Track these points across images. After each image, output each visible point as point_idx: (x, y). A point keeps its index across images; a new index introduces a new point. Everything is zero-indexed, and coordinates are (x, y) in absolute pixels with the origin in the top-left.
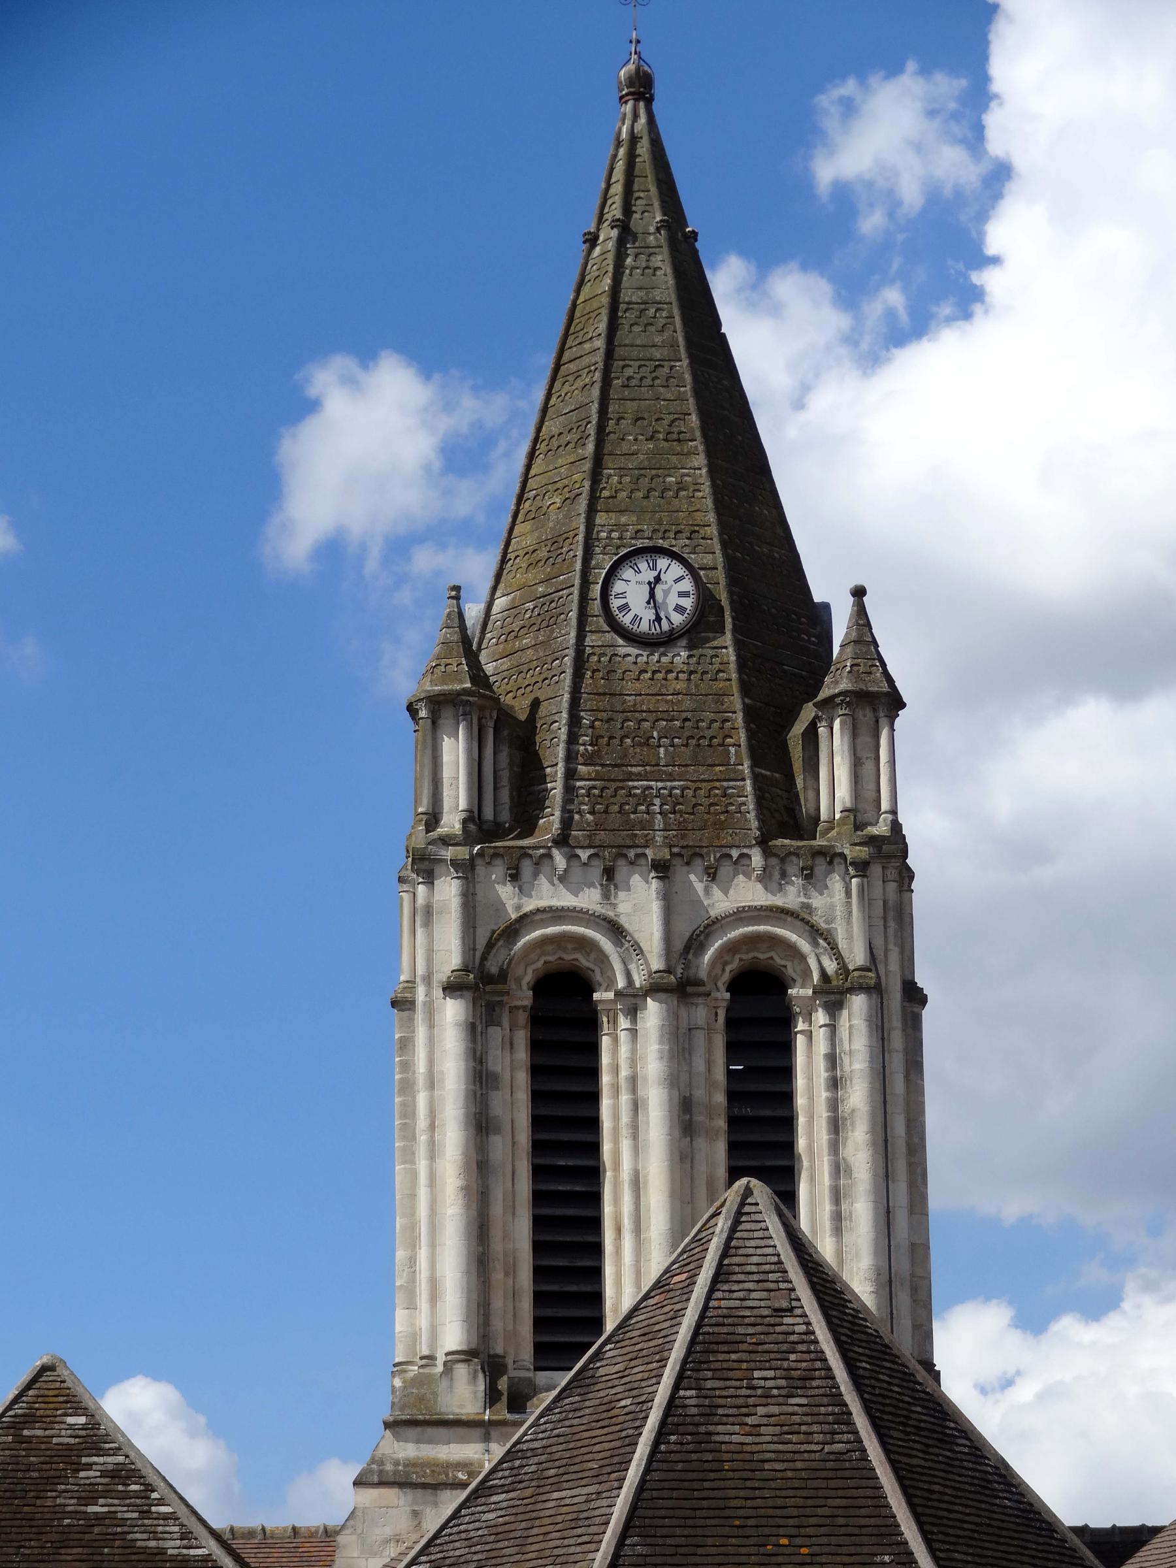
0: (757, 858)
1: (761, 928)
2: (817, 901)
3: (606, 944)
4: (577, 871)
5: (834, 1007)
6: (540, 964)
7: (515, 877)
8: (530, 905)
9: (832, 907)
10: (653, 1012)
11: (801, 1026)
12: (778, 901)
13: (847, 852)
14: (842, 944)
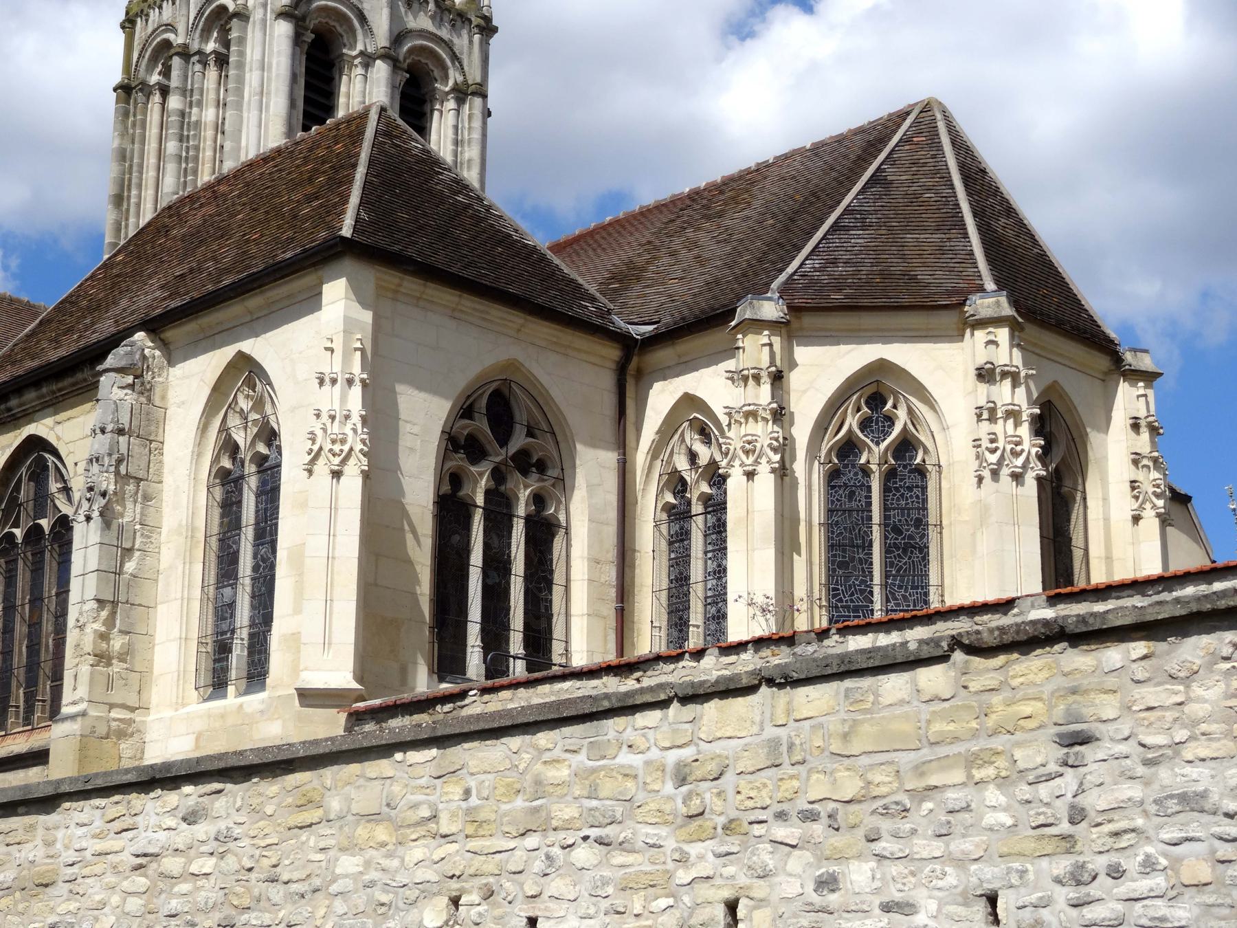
1: (430, 44)
2: (456, 40)
5: (460, 101)
6: (317, 22)
9: (462, 46)
10: (381, 69)
11: (438, 107)
12: (439, 33)
13: (473, 19)
14: (466, 68)
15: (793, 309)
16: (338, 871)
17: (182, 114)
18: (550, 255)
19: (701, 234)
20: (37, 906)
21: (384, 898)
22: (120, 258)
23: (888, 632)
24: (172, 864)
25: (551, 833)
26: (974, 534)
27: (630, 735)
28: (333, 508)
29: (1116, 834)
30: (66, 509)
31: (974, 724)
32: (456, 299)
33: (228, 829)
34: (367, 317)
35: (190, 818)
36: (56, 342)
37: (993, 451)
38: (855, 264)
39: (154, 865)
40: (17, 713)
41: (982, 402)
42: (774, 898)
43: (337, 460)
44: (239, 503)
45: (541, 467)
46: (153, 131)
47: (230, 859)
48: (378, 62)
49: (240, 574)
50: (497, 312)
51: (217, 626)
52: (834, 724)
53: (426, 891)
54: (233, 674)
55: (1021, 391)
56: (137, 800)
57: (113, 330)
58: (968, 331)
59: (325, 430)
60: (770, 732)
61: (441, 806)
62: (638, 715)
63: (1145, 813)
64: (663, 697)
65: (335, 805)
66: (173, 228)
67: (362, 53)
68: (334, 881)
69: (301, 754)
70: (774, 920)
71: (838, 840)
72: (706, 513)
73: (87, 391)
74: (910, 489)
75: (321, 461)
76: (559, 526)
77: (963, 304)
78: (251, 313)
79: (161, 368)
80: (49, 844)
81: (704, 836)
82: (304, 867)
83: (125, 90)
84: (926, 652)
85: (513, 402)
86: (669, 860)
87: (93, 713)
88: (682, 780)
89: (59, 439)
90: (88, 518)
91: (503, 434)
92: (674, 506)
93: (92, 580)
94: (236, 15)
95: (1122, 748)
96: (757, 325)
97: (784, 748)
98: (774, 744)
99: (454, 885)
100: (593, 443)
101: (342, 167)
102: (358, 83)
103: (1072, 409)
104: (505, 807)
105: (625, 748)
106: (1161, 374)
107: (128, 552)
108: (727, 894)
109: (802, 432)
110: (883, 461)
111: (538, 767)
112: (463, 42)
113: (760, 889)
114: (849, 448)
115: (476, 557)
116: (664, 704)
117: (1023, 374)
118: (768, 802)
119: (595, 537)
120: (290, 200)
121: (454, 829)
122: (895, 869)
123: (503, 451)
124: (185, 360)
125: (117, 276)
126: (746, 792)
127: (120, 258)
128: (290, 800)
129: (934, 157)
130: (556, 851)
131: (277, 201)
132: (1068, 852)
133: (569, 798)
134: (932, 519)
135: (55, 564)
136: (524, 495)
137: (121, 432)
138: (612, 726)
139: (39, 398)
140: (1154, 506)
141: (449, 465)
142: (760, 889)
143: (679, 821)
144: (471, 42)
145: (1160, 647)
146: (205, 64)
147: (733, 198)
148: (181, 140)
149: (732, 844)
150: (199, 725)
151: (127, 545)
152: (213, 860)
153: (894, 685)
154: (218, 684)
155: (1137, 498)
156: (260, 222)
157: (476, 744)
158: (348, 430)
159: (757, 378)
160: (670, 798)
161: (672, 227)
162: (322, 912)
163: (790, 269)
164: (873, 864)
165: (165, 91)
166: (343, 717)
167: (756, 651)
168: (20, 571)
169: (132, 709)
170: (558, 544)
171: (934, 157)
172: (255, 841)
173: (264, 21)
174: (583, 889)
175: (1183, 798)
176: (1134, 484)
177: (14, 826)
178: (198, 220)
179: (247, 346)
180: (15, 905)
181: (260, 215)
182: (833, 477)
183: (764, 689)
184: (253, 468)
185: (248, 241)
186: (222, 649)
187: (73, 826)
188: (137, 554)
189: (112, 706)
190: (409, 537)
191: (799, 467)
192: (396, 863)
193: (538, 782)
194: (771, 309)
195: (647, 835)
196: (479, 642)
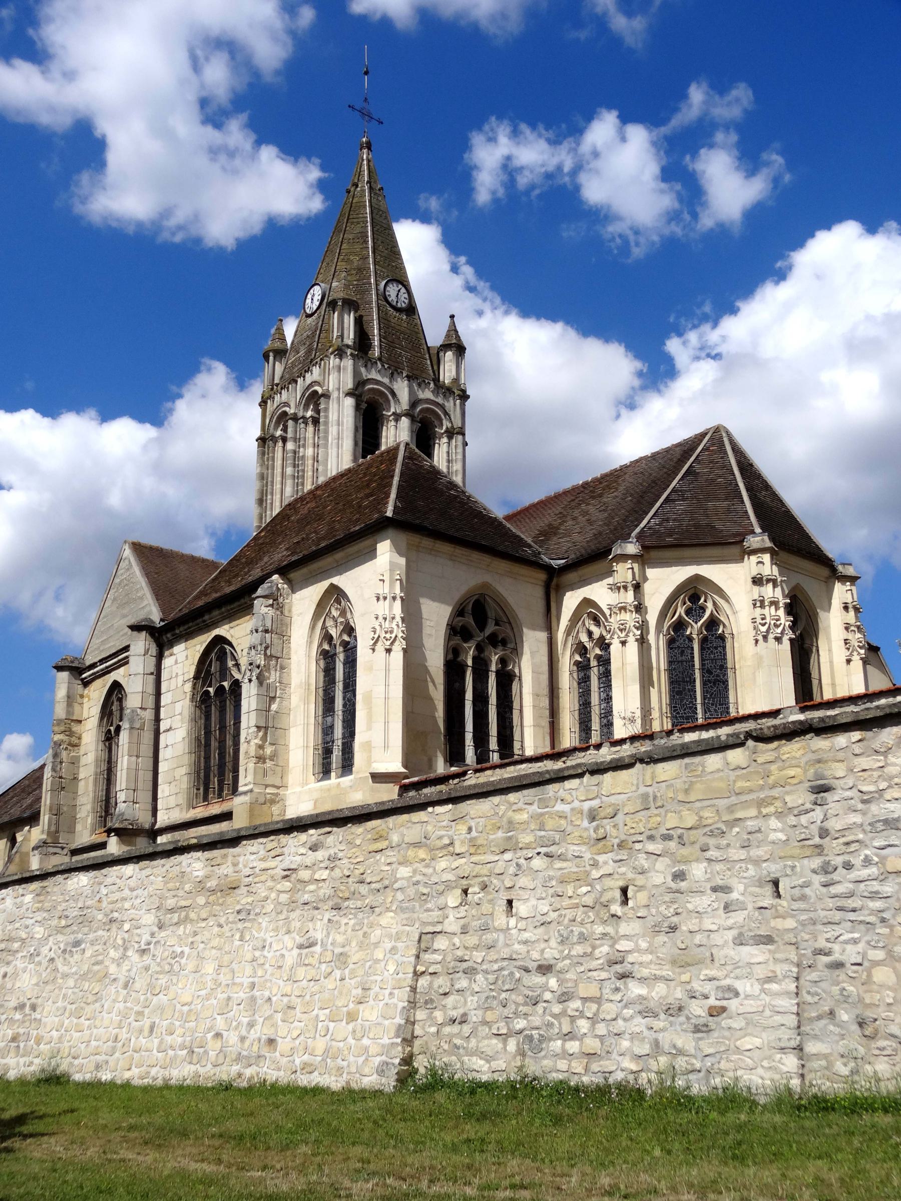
0: (432, 385)
2: (446, 404)
3: (390, 397)
4: (383, 371)
5: (450, 438)
7: (366, 366)
8: (370, 377)
10: (405, 422)
12: (436, 400)
15: (645, 548)
16: (398, 876)
17: (295, 452)
18: (504, 522)
19: (590, 507)
20: (230, 900)
21: (425, 891)
22: (263, 534)
23: (707, 730)
24: (304, 874)
25: (519, 851)
26: (754, 673)
27: (562, 794)
28: (387, 670)
29: (847, 844)
30: (237, 676)
31: (761, 782)
32: (452, 549)
33: (335, 854)
34: (402, 561)
35: (314, 848)
36: (229, 583)
37: (763, 625)
38: (679, 521)
39: (294, 875)
40: (214, 792)
41: (756, 597)
42: (649, 885)
43: (388, 643)
44: (334, 669)
45: (504, 642)
46: (278, 463)
47: (337, 871)
48: (403, 418)
49: (336, 709)
50: (476, 556)
51: (324, 739)
52: (679, 784)
53: (449, 886)
54: (334, 766)
55: (778, 590)
56: (283, 838)
57: (260, 574)
58: (746, 557)
59: (381, 626)
60: (643, 790)
61: (455, 837)
62: (566, 782)
63: (864, 831)
64: (580, 771)
65: (395, 838)
66: (292, 516)
67: (394, 414)
68: (396, 882)
69: (375, 810)
70: (649, 898)
71: (684, 851)
72: (599, 666)
73: (247, 609)
74: (716, 648)
75: (380, 643)
76: (515, 676)
77: (743, 541)
78: (337, 562)
79: (288, 595)
80: (235, 865)
81: (606, 851)
82: (379, 874)
83: (263, 440)
84: (731, 741)
85: (487, 607)
86: (587, 865)
87: (256, 790)
88: (593, 819)
89: (232, 636)
90: (250, 681)
91: (481, 624)
92: (580, 662)
93: (253, 715)
94: (323, 395)
95: (849, 794)
96: (624, 557)
97: (651, 799)
98: (645, 796)
99: (464, 882)
100: (533, 628)
101: (385, 477)
102: (392, 430)
103: (808, 599)
104: (492, 837)
105: (559, 801)
106: (859, 578)
107: (273, 699)
108: (621, 883)
109: (652, 618)
110: (700, 632)
111: (510, 813)
112: (451, 405)
113: (640, 880)
114: (679, 626)
115: (469, 695)
116: (580, 776)
117: (779, 580)
118: (643, 830)
119: (536, 681)
120: (357, 497)
121: (463, 850)
122: (718, 867)
123: (482, 634)
124: (301, 589)
125: (262, 544)
126: (630, 824)
127: (263, 534)
128: (370, 836)
129: (722, 458)
130: (522, 861)
131: (349, 498)
132: (819, 855)
133: (528, 831)
134: (729, 665)
135: (232, 707)
136: (495, 659)
137: (266, 631)
138: (551, 788)
139: (220, 614)
140: (859, 654)
141: (452, 643)
142: (640, 880)
143: (592, 842)
144: (455, 404)
145: (869, 734)
146: (306, 423)
147: (607, 486)
148: (294, 467)
149: (623, 855)
150: (316, 795)
151: (272, 695)
152: (327, 871)
153: (713, 761)
154: (325, 771)
155: (848, 649)
156: (340, 510)
157: (474, 801)
158: (394, 625)
159: (625, 588)
160: (586, 829)
161: (573, 504)
162: (390, 899)
163: (642, 525)
164: (705, 864)
165: (284, 440)
166: (397, 788)
167: (631, 744)
168: (213, 711)
169: (278, 788)
170: (515, 686)
171: (722, 458)
172: (351, 860)
173: (339, 398)
174: (538, 883)
175: (886, 822)
176: (846, 641)
177: (215, 855)
178: (305, 511)
179: (336, 580)
180: (218, 900)
181: (340, 506)
182: (671, 643)
183: (638, 765)
184: (341, 649)
185: (334, 521)
186: (327, 752)
187: (248, 854)
188: (278, 700)
189: (267, 786)
190: (430, 685)
191: (651, 638)
192: (431, 870)
193: (510, 822)
194: (632, 548)
195: (574, 851)
196: (472, 743)
